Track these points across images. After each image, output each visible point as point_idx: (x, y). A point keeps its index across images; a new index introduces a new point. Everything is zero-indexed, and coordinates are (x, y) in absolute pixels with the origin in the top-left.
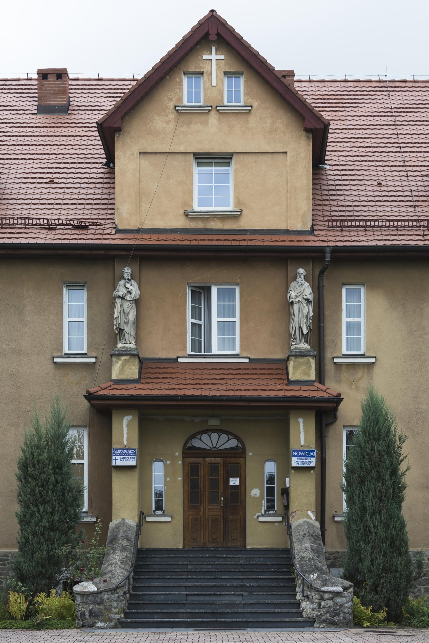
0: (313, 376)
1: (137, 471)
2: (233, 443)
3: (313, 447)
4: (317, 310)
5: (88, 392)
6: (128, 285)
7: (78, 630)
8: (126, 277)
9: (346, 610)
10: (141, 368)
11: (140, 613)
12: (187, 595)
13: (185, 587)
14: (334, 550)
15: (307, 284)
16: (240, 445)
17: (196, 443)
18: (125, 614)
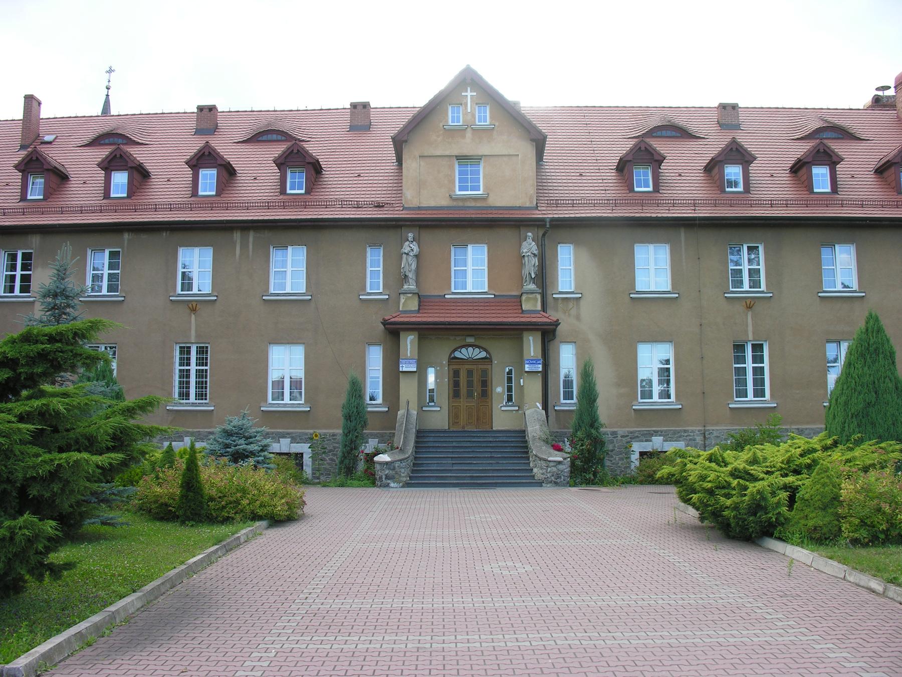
0: (539, 307)
1: (417, 374)
2: (483, 354)
3: (540, 357)
4: (541, 261)
5: (384, 319)
6: (411, 245)
7: (378, 489)
8: (410, 240)
9: (566, 474)
10: (420, 302)
11: (421, 477)
12: (453, 464)
13: (452, 458)
14: (555, 430)
15: (534, 243)
16: (488, 356)
17: (457, 354)
18: (410, 477)
